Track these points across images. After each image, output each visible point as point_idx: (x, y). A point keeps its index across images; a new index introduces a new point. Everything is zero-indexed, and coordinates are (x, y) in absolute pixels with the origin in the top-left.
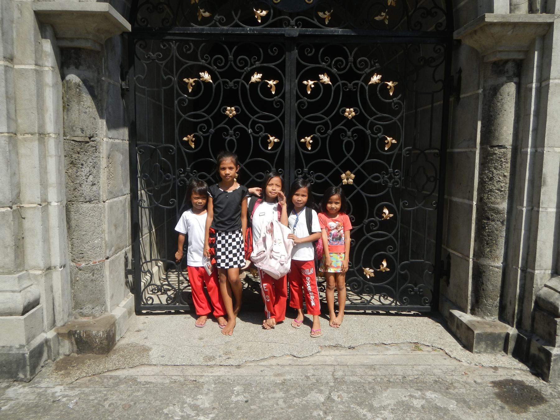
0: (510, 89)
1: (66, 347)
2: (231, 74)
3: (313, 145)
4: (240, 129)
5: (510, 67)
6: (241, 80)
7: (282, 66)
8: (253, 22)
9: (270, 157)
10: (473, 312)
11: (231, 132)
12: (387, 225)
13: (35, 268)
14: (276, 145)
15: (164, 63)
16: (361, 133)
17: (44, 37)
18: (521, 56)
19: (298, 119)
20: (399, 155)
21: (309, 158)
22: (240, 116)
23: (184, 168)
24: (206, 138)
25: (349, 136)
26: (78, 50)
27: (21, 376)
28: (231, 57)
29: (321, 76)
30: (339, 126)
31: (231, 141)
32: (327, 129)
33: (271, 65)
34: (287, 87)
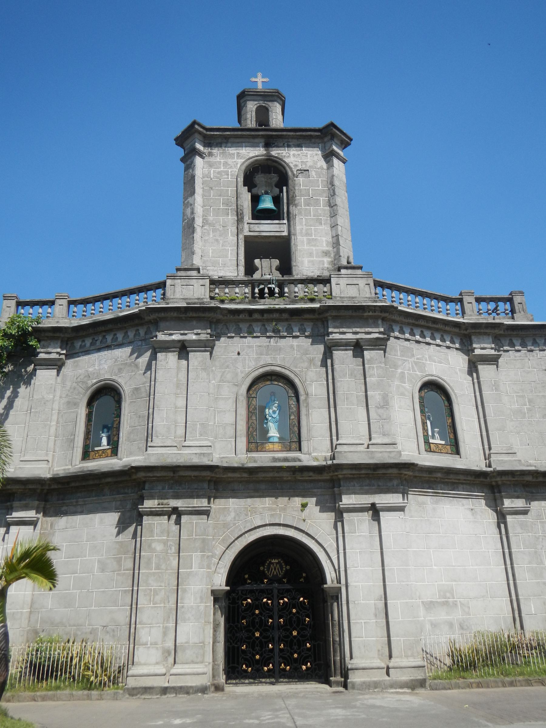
0: (335, 604)
1: (213, 689)
2: (257, 599)
3: (283, 622)
4: (260, 618)
5: (335, 597)
6: (260, 601)
7: (273, 596)
8: (264, 583)
9: (270, 626)
10: (334, 677)
11: (257, 618)
12: (309, 649)
13: (207, 662)
14: (271, 622)
15: (237, 597)
16: (298, 617)
17: (212, 596)
18: (336, 594)
19: (278, 613)
20: (310, 624)
21: (282, 626)
22: (260, 613)
23: (242, 631)
24: (249, 621)
25: (294, 619)
26: (218, 598)
27: (206, 692)
28: (257, 594)
29: (285, 599)
30: (291, 615)
31: (257, 622)
32: (287, 616)
33: (269, 596)
34: (274, 603)
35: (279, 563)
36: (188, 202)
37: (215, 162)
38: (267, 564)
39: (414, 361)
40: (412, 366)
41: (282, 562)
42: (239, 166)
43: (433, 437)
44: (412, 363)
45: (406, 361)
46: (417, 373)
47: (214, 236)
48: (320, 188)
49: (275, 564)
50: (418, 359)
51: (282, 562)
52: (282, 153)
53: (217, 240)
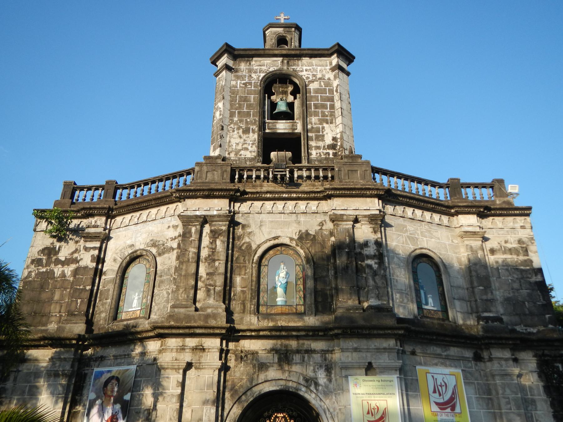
35: (284, 417)
36: (218, 107)
37: (242, 76)
38: (273, 418)
39: (407, 236)
40: (406, 240)
41: (287, 416)
42: (260, 78)
43: (427, 304)
44: (406, 238)
45: (400, 235)
46: (411, 246)
47: (238, 133)
48: (328, 95)
49: (280, 418)
50: (411, 234)
51: (287, 416)
52: (297, 68)
53: (240, 137)
